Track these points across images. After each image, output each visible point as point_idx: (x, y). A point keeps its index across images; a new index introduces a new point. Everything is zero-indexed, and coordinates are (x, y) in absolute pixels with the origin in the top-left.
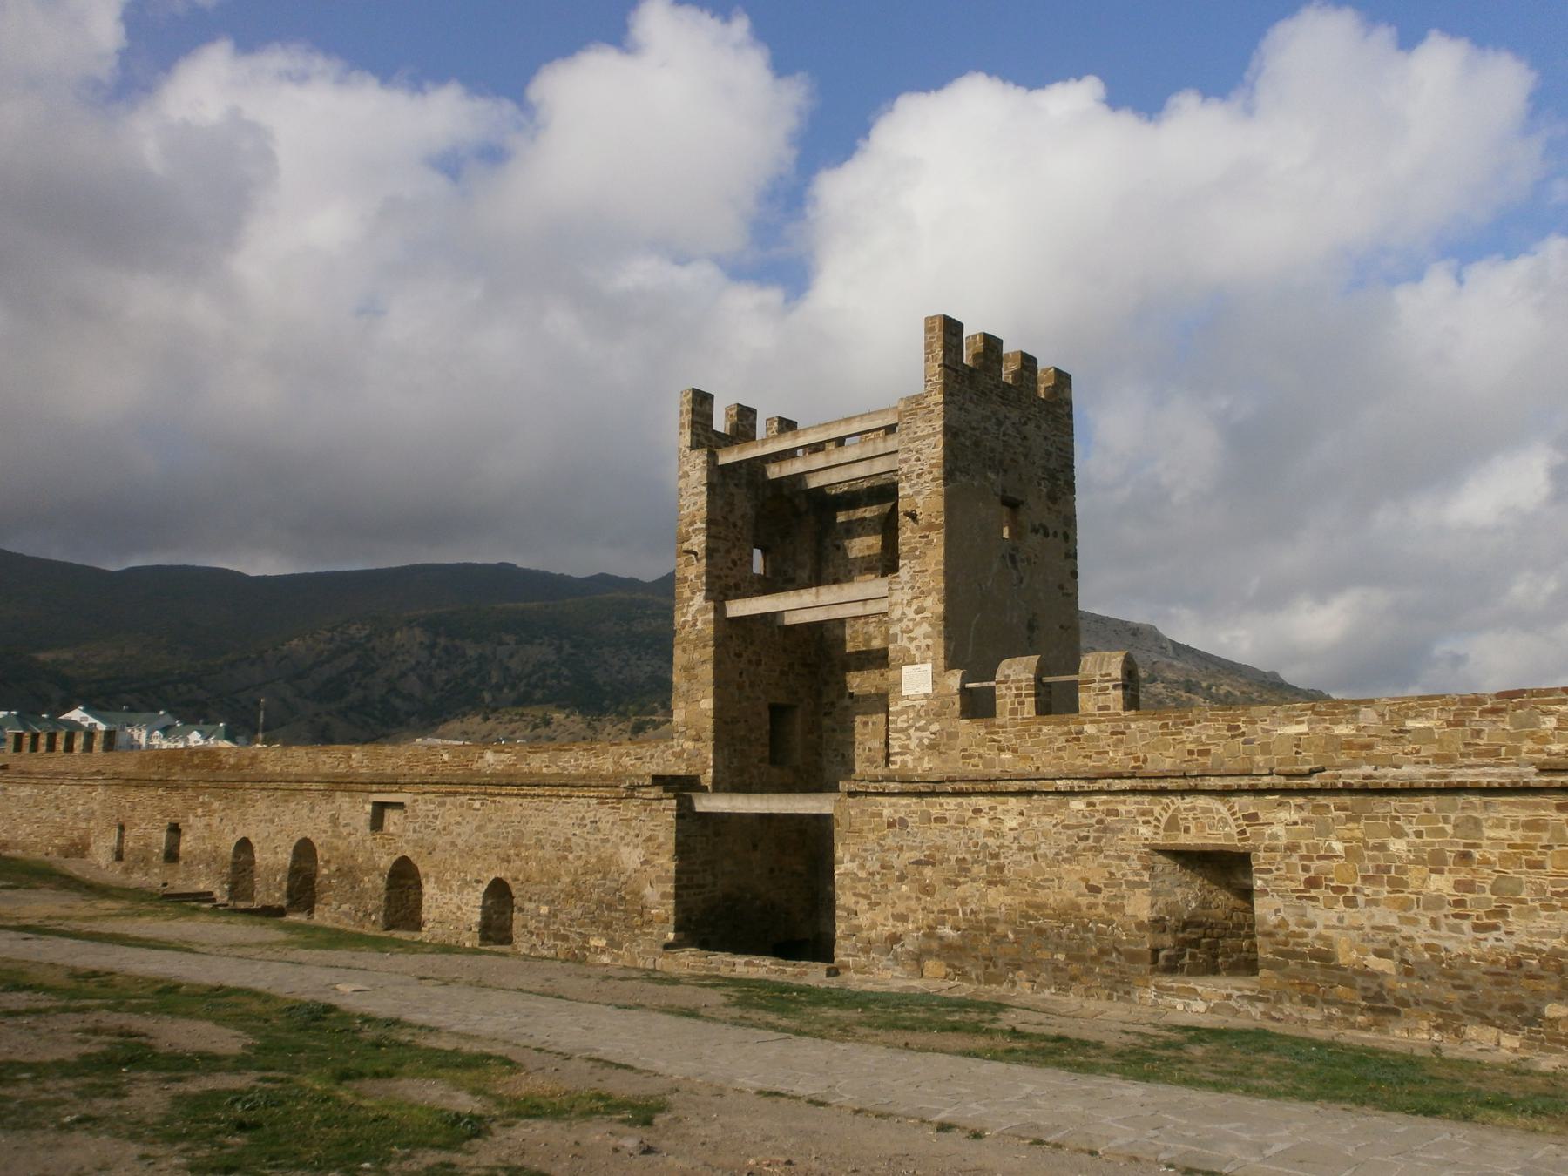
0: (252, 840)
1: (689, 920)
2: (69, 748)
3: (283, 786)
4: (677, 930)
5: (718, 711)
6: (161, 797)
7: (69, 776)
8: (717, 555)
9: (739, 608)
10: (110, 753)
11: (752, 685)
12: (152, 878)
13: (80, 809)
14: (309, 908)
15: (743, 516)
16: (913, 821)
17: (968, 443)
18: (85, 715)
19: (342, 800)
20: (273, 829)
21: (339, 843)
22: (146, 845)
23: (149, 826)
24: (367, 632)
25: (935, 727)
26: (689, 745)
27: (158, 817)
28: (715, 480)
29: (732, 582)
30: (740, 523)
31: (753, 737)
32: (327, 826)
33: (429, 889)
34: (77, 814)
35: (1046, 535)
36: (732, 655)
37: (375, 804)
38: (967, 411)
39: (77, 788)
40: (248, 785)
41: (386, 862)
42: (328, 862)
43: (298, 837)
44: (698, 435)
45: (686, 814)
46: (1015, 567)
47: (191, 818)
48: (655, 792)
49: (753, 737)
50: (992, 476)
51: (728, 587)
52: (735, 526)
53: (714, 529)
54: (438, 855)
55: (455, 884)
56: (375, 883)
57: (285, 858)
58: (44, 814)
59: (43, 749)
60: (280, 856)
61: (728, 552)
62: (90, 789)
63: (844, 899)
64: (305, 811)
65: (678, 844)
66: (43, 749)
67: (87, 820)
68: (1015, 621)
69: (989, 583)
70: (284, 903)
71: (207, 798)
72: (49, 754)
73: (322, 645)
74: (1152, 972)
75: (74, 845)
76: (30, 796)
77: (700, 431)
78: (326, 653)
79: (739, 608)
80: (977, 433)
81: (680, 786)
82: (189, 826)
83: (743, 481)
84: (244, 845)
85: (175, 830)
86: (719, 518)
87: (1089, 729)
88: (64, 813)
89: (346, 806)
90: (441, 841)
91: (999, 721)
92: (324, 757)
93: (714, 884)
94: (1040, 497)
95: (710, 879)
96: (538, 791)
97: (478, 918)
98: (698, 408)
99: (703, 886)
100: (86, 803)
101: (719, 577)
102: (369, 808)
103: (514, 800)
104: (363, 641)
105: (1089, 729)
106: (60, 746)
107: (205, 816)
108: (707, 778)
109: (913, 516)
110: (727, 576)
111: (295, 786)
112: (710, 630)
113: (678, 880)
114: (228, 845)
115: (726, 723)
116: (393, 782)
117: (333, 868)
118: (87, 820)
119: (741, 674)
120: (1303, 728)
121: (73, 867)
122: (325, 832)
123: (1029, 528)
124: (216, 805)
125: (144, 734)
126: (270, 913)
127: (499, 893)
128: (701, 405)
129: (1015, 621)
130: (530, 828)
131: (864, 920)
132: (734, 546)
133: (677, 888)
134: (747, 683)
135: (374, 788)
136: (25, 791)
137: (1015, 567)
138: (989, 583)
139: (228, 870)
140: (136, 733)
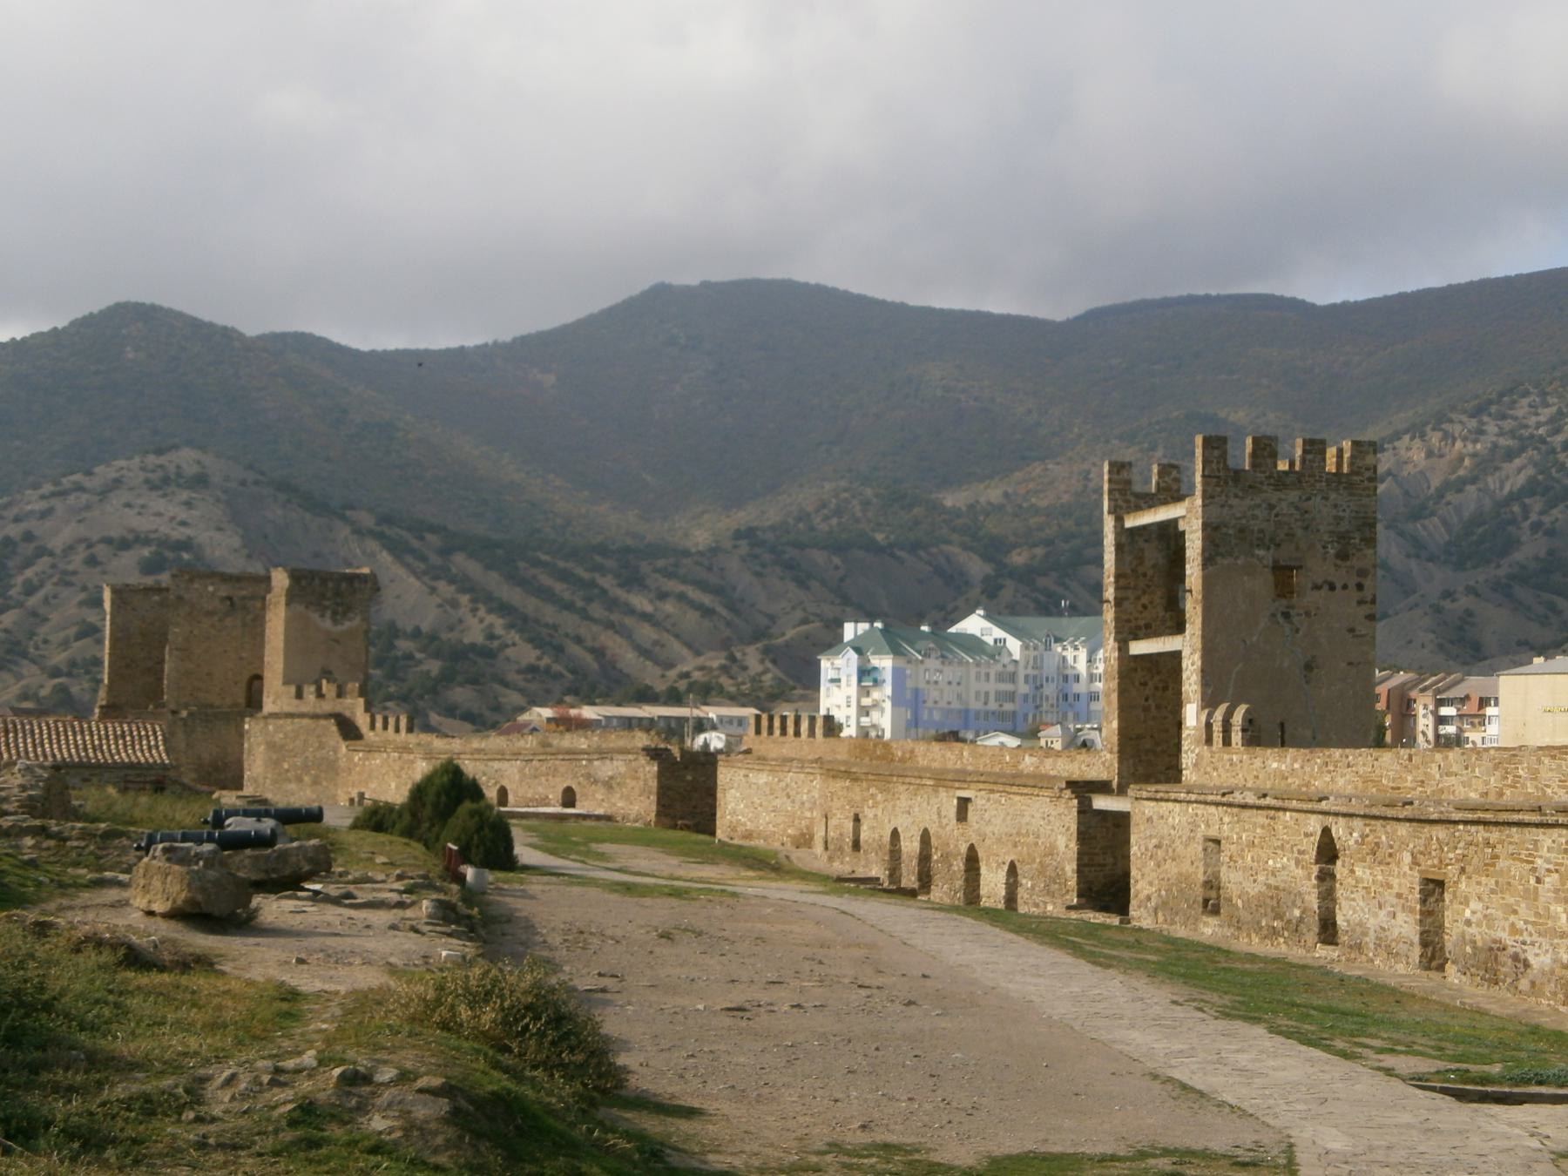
1: (1090, 889)
2: (797, 734)
3: (913, 780)
4: (1079, 896)
5: (1120, 729)
6: (848, 788)
7: (795, 763)
8: (1126, 604)
9: (1139, 648)
10: (832, 739)
11: (1158, 707)
12: (841, 867)
13: (805, 797)
14: (928, 893)
15: (1154, 566)
16: (1155, 818)
17: (1231, 532)
18: (986, 624)
19: (943, 793)
20: (910, 820)
22: (841, 835)
24: (1554, 409)
25: (1197, 751)
26: (1108, 756)
28: (1123, 540)
29: (1142, 623)
30: (1150, 573)
31: (1159, 749)
32: (935, 817)
33: (983, 870)
34: (803, 803)
36: (1137, 684)
37: (960, 799)
38: (1231, 507)
39: (802, 776)
40: (895, 779)
44: (1116, 500)
45: (1085, 810)
46: (1291, 622)
47: (866, 809)
48: (1068, 793)
49: (1159, 749)
50: (1261, 553)
51: (1138, 628)
52: (1145, 575)
53: (1122, 582)
55: (994, 865)
56: (959, 865)
58: (777, 802)
59: (777, 732)
61: (1138, 598)
62: (811, 777)
63: (1134, 872)
64: (925, 804)
65: (1079, 833)
66: (764, 732)
67: (811, 810)
68: (1286, 665)
69: (1255, 638)
70: (916, 886)
72: (783, 739)
73: (1459, 444)
74: (1203, 913)
75: (803, 835)
76: (766, 783)
77: (1117, 495)
78: (1467, 462)
79: (1139, 648)
81: (1083, 789)
83: (1154, 536)
85: (857, 819)
86: (1129, 571)
88: (793, 802)
90: (989, 830)
91: (1214, 748)
92: (949, 754)
93: (1115, 864)
94: (1325, 559)
95: (1110, 860)
96: (1025, 790)
97: (1003, 893)
98: (1116, 477)
99: (1105, 865)
100: (809, 791)
101: (1128, 621)
102: (955, 801)
104: (1541, 431)
106: (791, 730)
108: (1115, 784)
109: (1190, 591)
110: (1136, 619)
111: (918, 781)
112: (1116, 667)
113: (1078, 859)
115: (1131, 739)
118: (811, 810)
119: (1147, 700)
120: (1275, 765)
121: (801, 859)
123: (1310, 585)
124: (879, 797)
125: (1083, 655)
126: (912, 893)
127: (1012, 870)
128: (1118, 472)
129: (1286, 665)
130: (1024, 821)
131: (1139, 886)
132: (1144, 592)
133: (1078, 865)
134: (1153, 707)
135: (957, 785)
136: (763, 778)
137: (1291, 622)
138: (1255, 638)
139: (887, 858)
140: (1069, 654)
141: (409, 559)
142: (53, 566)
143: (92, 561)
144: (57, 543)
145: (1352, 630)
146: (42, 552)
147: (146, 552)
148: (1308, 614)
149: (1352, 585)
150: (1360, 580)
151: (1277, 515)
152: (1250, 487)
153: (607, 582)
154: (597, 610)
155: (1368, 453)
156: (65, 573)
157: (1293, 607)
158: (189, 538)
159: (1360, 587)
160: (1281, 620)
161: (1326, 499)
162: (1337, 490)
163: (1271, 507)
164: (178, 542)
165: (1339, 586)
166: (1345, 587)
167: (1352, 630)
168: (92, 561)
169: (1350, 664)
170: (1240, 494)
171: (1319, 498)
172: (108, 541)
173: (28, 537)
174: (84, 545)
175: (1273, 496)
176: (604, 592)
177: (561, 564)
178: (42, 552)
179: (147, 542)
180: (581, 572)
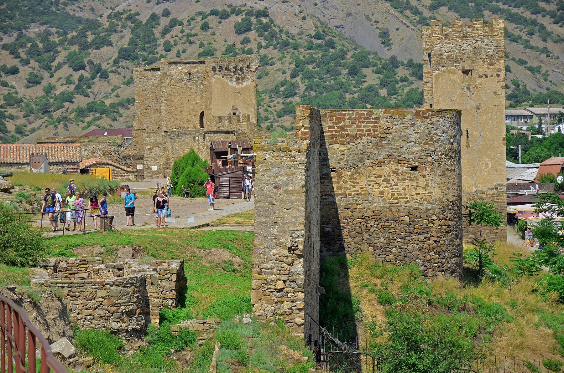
17: (445, 57)
35: (487, 77)
80: (449, 53)
141: (408, 13)
142: (182, 32)
143: (205, 27)
144: (183, 17)
145: (495, 93)
146: (174, 23)
147: (239, 19)
148: (477, 87)
149: (495, 75)
150: (498, 73)
151: (463, 50)
152: (452, 39)
153: (546, 22)
154: (536, 41)
155: (501, 23)
156: (190, 35)
157: (471, 85)
158: (266, 8)
159: (498, 76)
160: (466, 90)
161: (484, 42)
162: (488, 38)
163: (461, 47)
164: (259, 11)
165: (489, 76)
166: (492, 76)
167: (495, 93)
168: (205, 27)
169: (494, 106)
170: (448, 42)
171: (481, 42)
172: (214, 13)
173: (166, 13)
174: (200, 17)
175: (460, 42)
176: (543, 27)
177: (514, 10)
178: (174, 23)
179: (239, 13)
180: (528, 15)
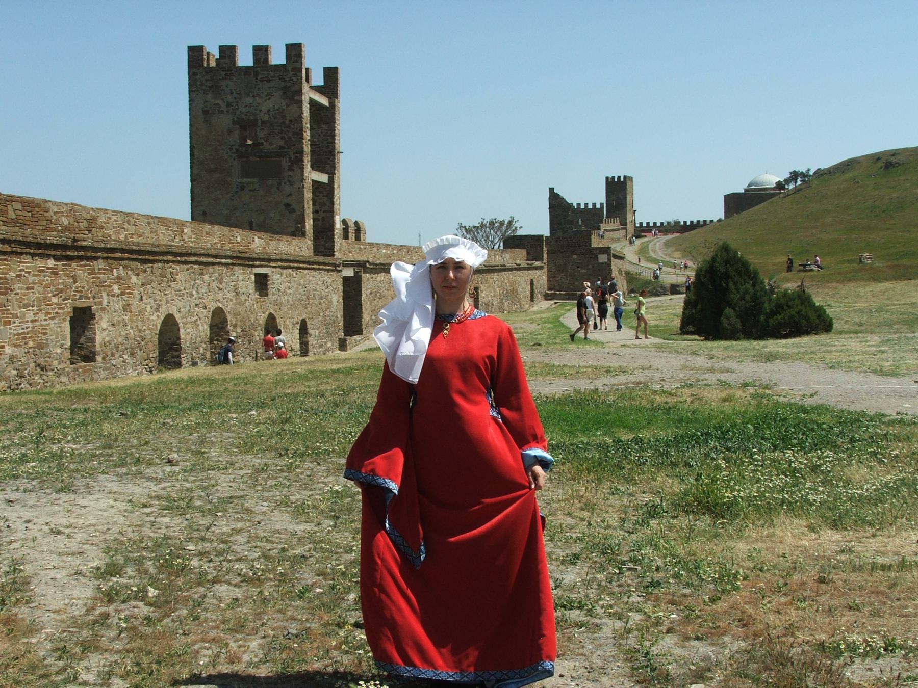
0: (177, 316)
19: (238, 270)
21: (240, 309)
23: (41, 316)
27: (55, 300)
32: (230, 295)
37: (257, 275)
41: (262, 318)
42: (235, 326)
43: (212, 306)
54: (285, 309)
57: (204, 329)
60: (201, 328)
71: (122, 271)
82: (103, 309)
84: (170, 324)
87: (362, 247)
89: (241, 278)
96: (315, 266)
102: (253, 277)
103: (306, 271)
105: (362, 247)
107: (123, 294)
114: (157, 320)
116: (267, 260)
117: (239, 330)
120: (384, 251)
122: (231, 300)
124: (134, 279)
